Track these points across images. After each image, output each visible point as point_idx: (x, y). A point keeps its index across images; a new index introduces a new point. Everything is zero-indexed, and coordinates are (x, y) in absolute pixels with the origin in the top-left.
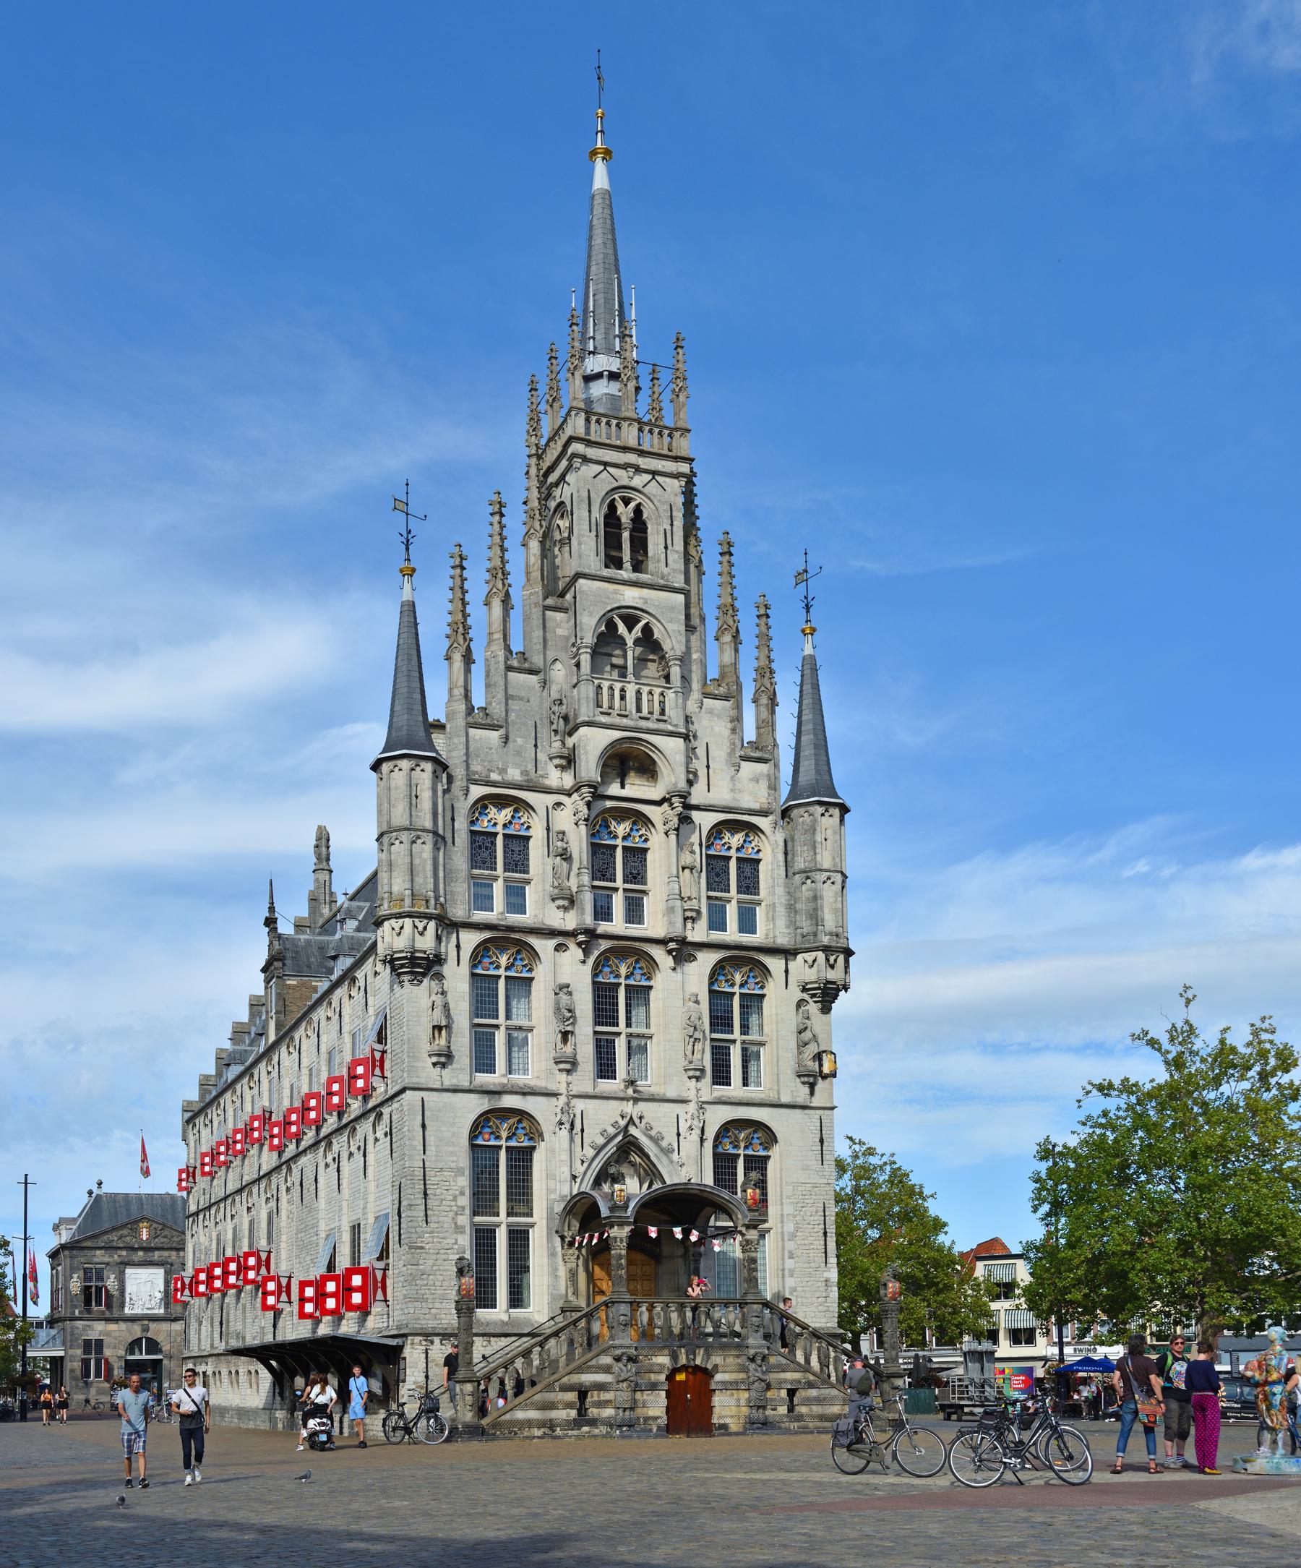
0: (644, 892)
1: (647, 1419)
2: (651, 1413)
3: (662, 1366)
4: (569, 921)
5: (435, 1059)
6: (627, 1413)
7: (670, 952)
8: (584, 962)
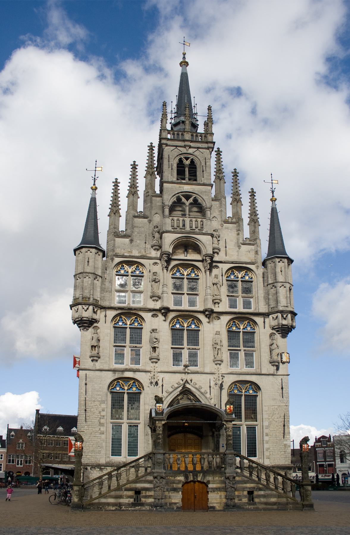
0: (197, 295)
1: (171, 504)
2: (173, 501)
3: (180, 481)
4: (158, 305)
5: (92, 359)
6: (160, 501)
7: (206, 316)
8: (165, 320)
